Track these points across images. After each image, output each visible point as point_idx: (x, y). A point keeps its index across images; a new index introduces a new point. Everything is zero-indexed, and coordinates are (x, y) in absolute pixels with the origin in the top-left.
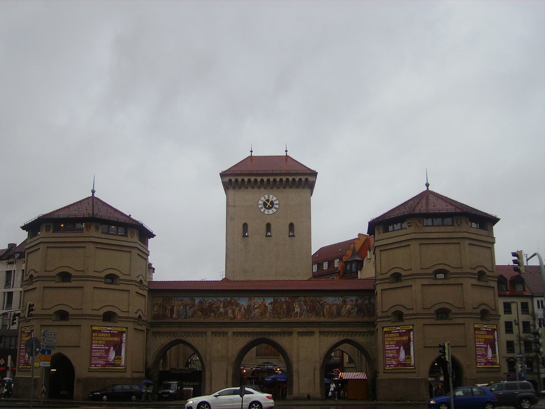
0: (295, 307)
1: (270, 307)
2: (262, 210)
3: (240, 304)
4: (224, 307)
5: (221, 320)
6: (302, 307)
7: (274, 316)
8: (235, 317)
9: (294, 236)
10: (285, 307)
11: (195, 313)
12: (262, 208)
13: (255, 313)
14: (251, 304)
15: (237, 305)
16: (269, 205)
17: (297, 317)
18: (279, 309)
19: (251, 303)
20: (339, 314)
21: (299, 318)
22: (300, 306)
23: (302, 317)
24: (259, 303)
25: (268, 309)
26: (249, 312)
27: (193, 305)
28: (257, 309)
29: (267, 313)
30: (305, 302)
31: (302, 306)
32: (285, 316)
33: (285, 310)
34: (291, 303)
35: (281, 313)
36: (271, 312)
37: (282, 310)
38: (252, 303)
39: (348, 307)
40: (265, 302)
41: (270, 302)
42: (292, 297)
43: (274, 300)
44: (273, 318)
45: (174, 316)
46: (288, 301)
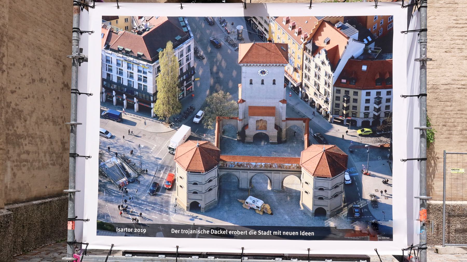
1: (263, 166)
2: (260, 75)
4: (246, 165)
5: (245, 168)
8: (250, 167)
9: (275, 84)
10: (269, 165)
11: (235, 166)
12: (260, 74)
15: (251, 164)
16: (263, 72)
20: (290, 168)
22: (275, 165)
27: (235, 164)
30: (277, 165)
39: (293, 166)
45: (227, 166)
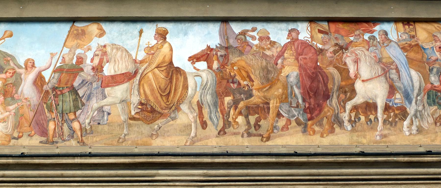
0: (356, 77)
3: (13, 58)
6: (394, 75)
7: (227, 124)
13: (106, 109)
14: (80, 60)
17: (373, 128)
18: (257, 83)
19: (78, 51)
21: (385, 136)
23: (401, 130)
24: (130, 55)
25: (186, 87)
26: (69, 98)
28: (122, 82)
29: (184, 107)
31: (398, 71)
32: (293, 119)
33: (297, 91)
34: (329, 54)
35: (273, 104)
36: (209, 98)
37: (278, 91)
38: (90, 55)
40: (171, 50)
41: (204, 47)
42: (330, 20)
43: (224, 35)
44: (222, 132)
46: (305, 45)
